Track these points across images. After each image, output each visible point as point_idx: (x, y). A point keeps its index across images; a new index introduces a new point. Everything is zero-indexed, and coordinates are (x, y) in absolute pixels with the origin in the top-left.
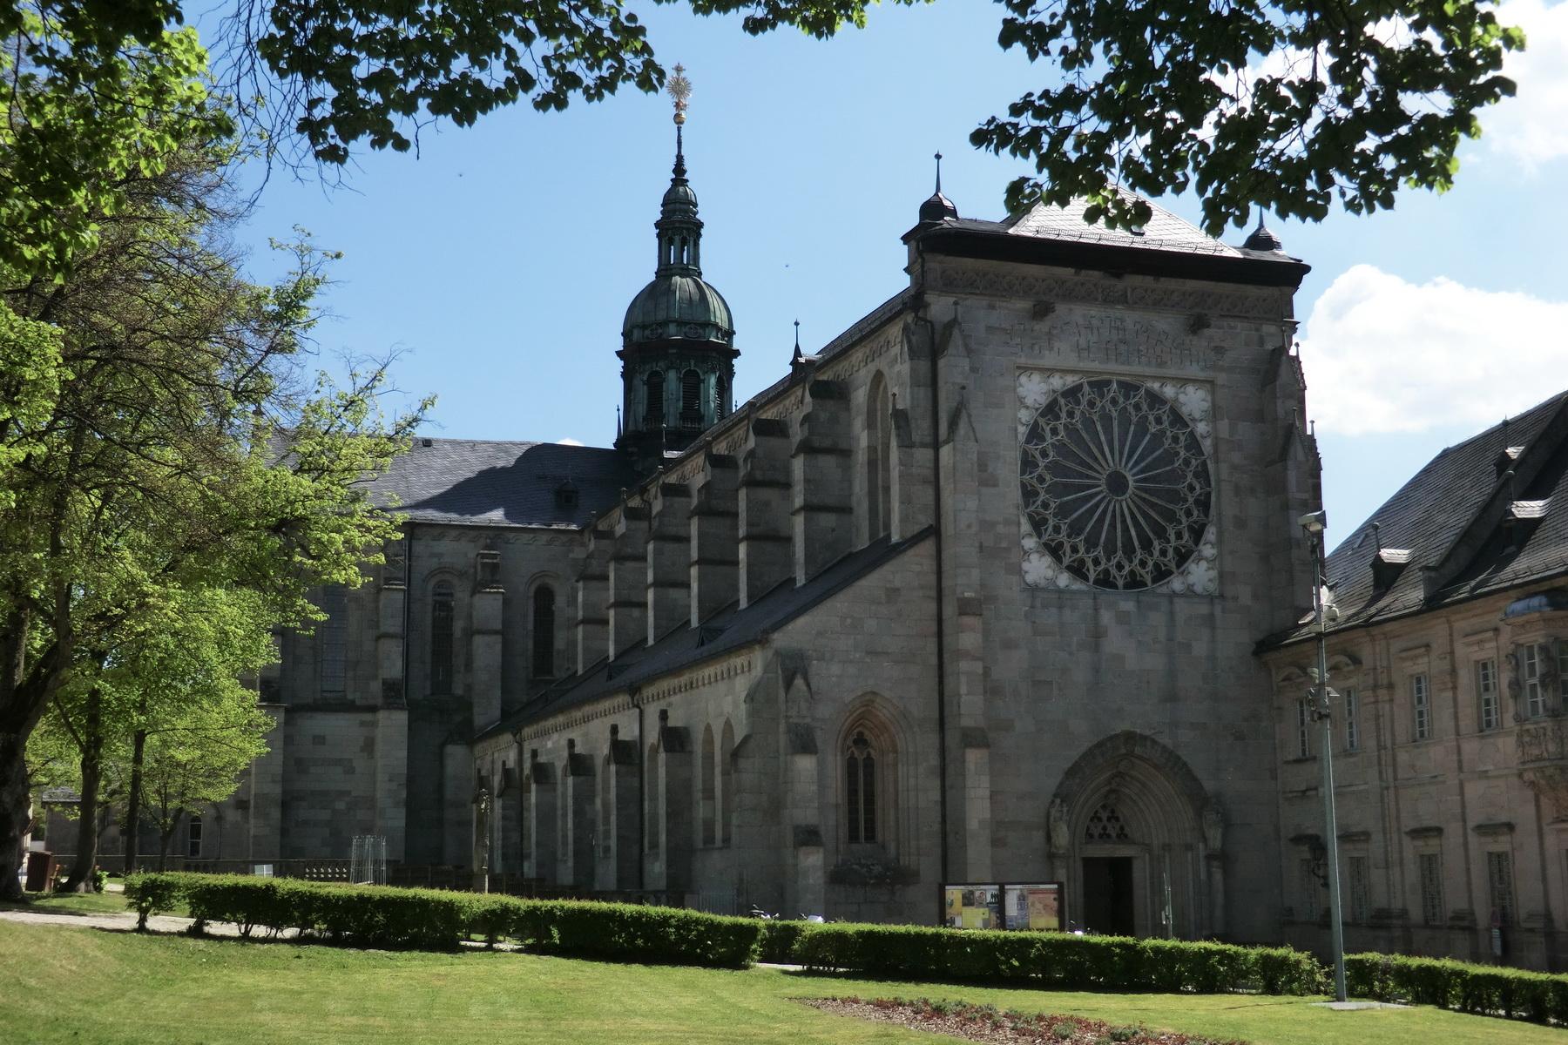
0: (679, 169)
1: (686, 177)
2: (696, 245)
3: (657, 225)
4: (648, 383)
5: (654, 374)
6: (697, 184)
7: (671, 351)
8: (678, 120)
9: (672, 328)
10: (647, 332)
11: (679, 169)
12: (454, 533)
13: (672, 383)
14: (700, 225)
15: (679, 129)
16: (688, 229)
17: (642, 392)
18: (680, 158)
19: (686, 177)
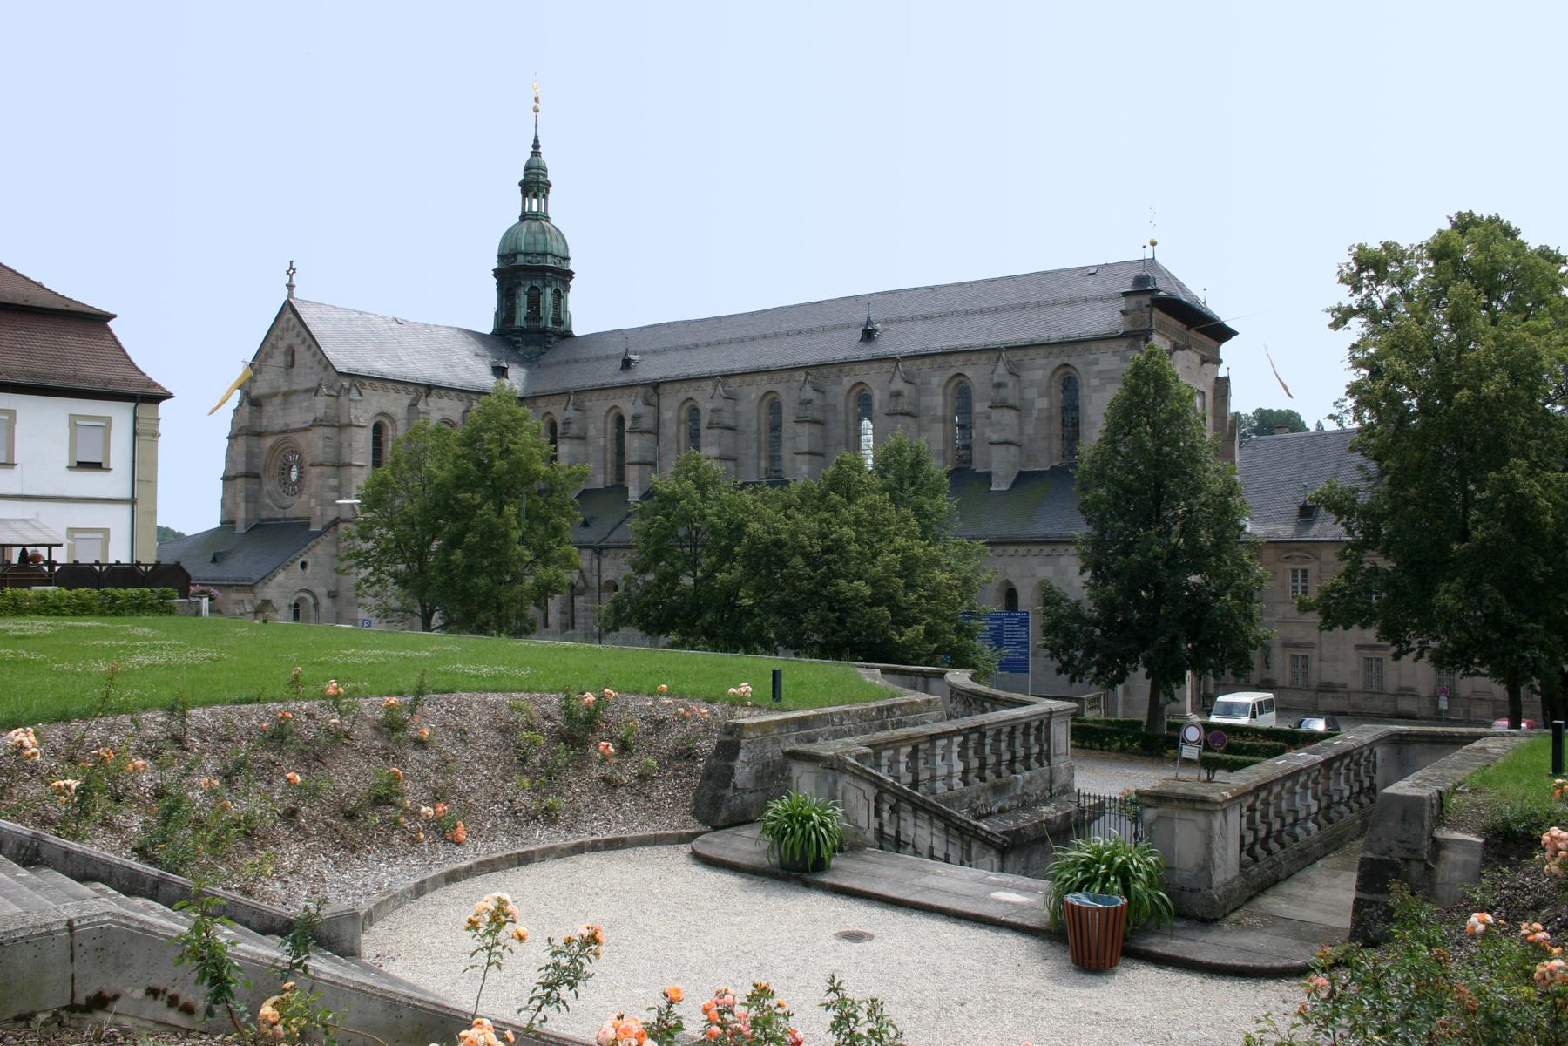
0: (536, 145)
1: (540, 150)
2: (544, 196)
3: (520, 184)
4: (528, 294)
5: (532, 288)
6: (546, 157)
7: (548, 274)
8: (536, 111)
9: (549, 258)
10: (529, 258)
11: (536, 145)
12: (453, 394)
13: (548, 296)
14: (550, 185)
17: (522, 301)
18: (536, 137)
19: (540, 150)
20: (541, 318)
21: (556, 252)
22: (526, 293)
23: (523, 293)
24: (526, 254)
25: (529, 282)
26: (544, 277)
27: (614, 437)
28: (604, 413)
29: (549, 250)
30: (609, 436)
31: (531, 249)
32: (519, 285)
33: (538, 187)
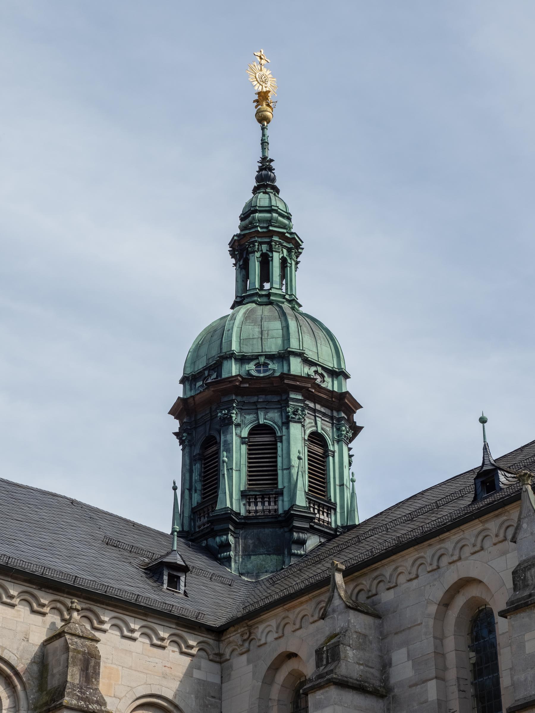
7: (292, 396)
8: (262, 119)
10: (251, 367)
15: (263, 129)
16: (289, 250)
20: (281, 493)
21: (311, 355)
22: (243, 441)
23: (236, 441)
24: (243, 359)
25: (250, 417)
26: (282, 406)
27: (468, 675)
28: (433, 609)
29: (294, 345)
30: (452, 674)
31: (248, 350)
32: (227, 422)
33: (269, 243)
